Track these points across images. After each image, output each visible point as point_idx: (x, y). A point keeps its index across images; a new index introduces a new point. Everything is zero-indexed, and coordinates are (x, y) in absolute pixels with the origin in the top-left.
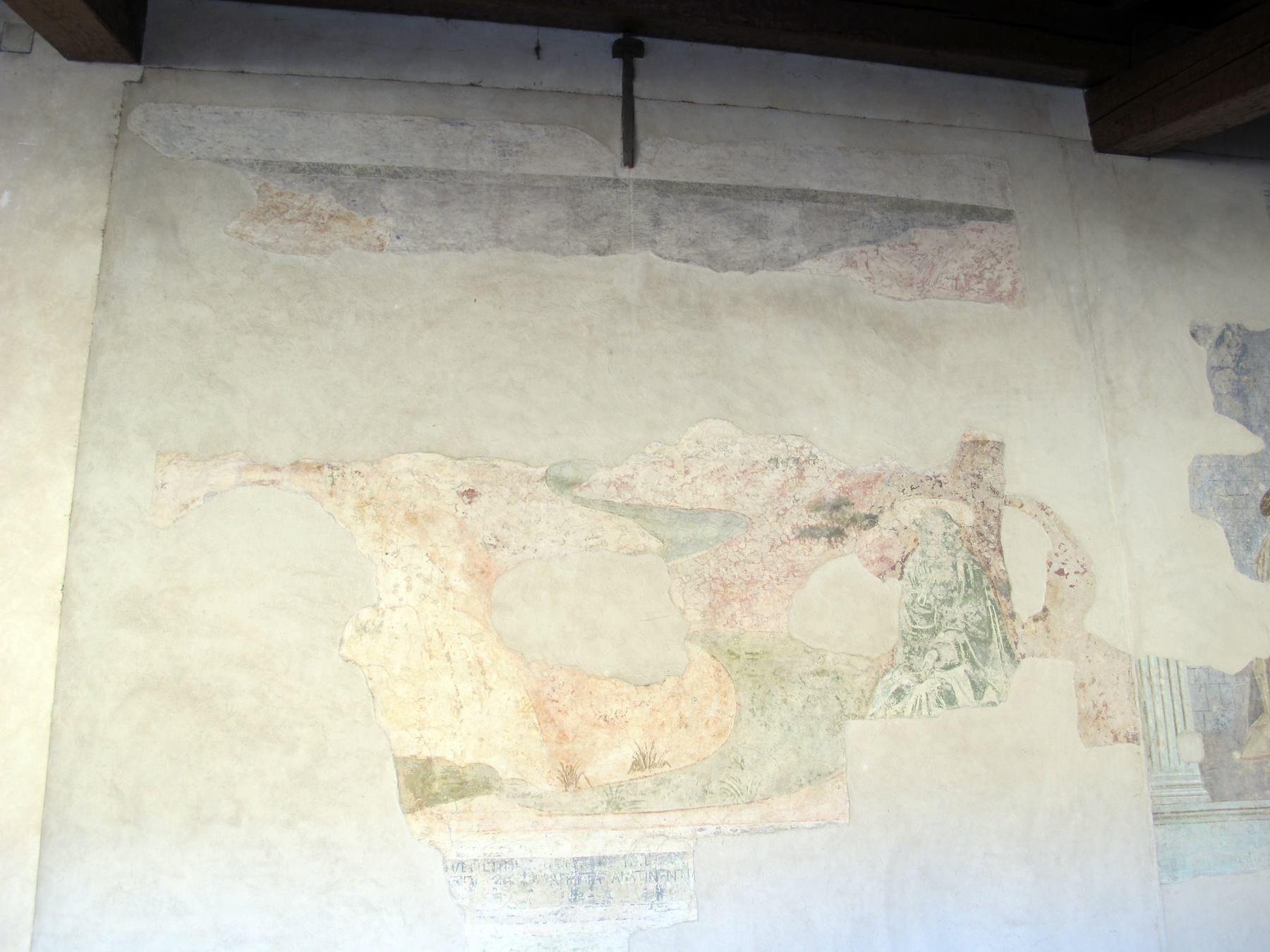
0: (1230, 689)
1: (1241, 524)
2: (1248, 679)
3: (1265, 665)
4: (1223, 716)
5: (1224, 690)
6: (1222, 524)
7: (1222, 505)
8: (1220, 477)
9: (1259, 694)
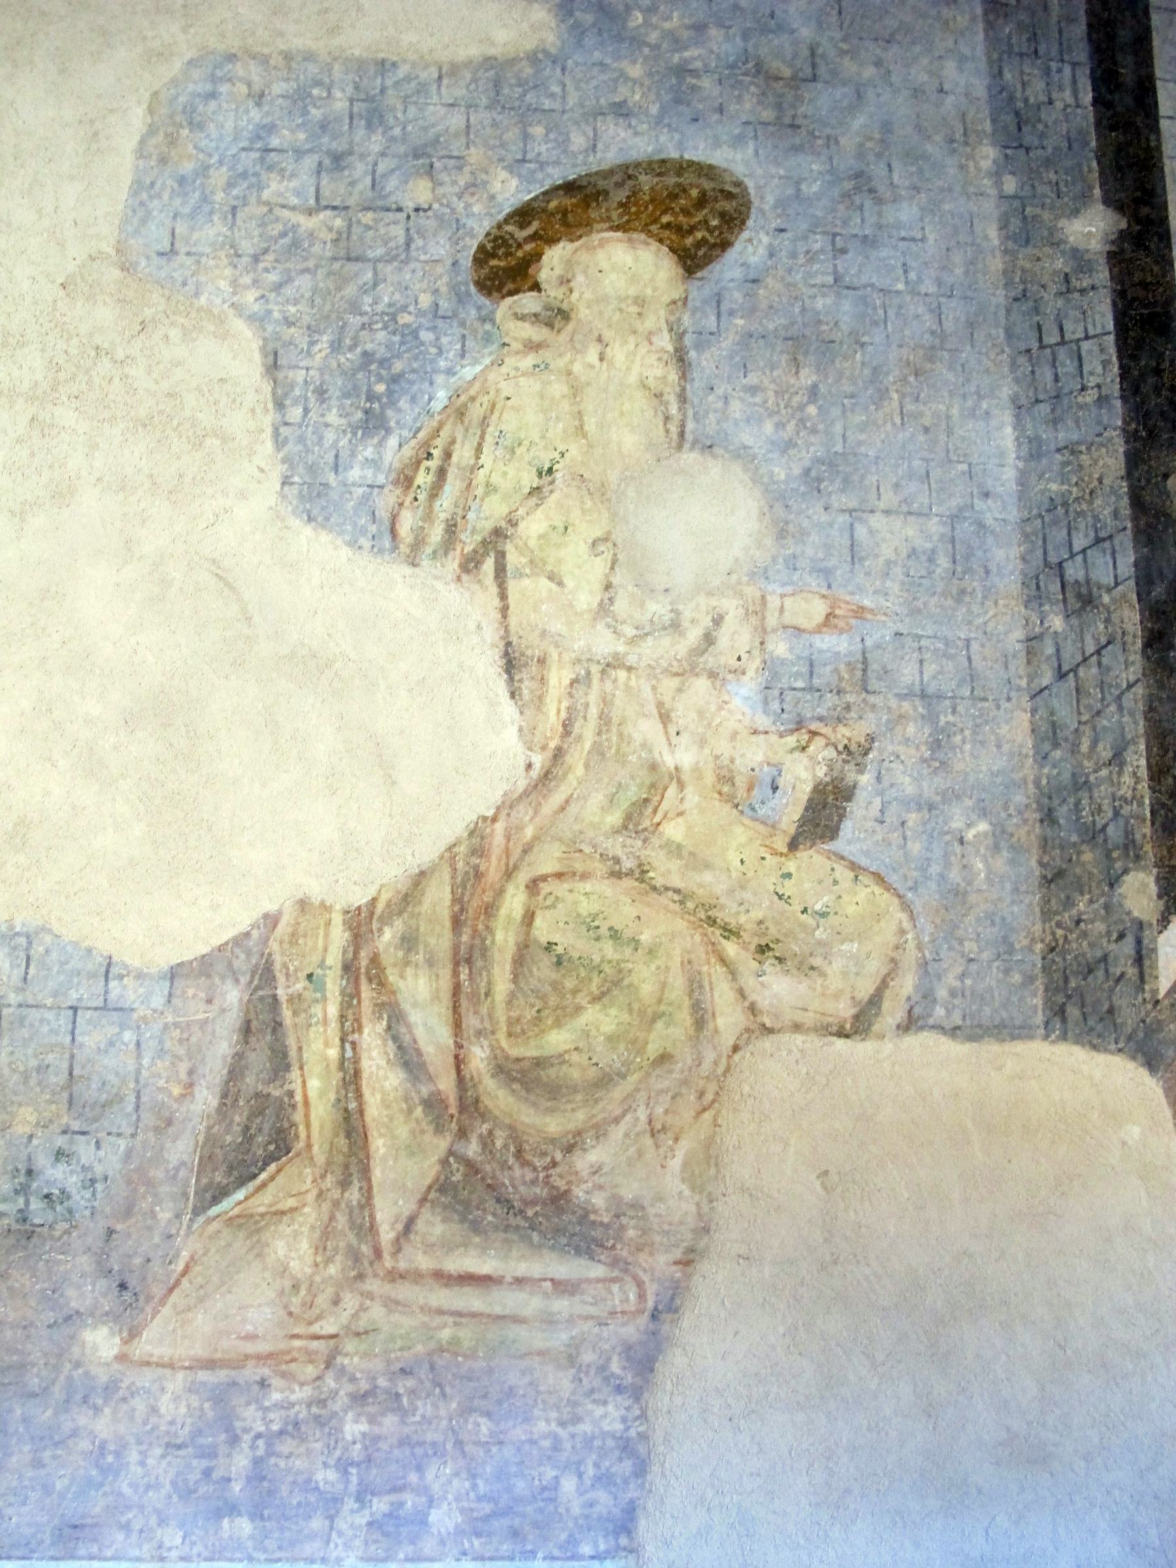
0: (128, 1036)
1: (355, 321)
2: (233, 996)
3: (339, 936)
4: (60, 1155)
5: (91, 1039)
6: (258, 320)
7: (286, 241)
8: (302, 136)
9: (281, 1062)
